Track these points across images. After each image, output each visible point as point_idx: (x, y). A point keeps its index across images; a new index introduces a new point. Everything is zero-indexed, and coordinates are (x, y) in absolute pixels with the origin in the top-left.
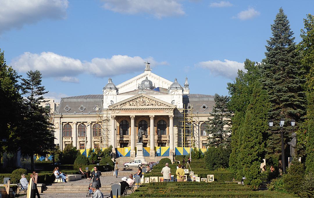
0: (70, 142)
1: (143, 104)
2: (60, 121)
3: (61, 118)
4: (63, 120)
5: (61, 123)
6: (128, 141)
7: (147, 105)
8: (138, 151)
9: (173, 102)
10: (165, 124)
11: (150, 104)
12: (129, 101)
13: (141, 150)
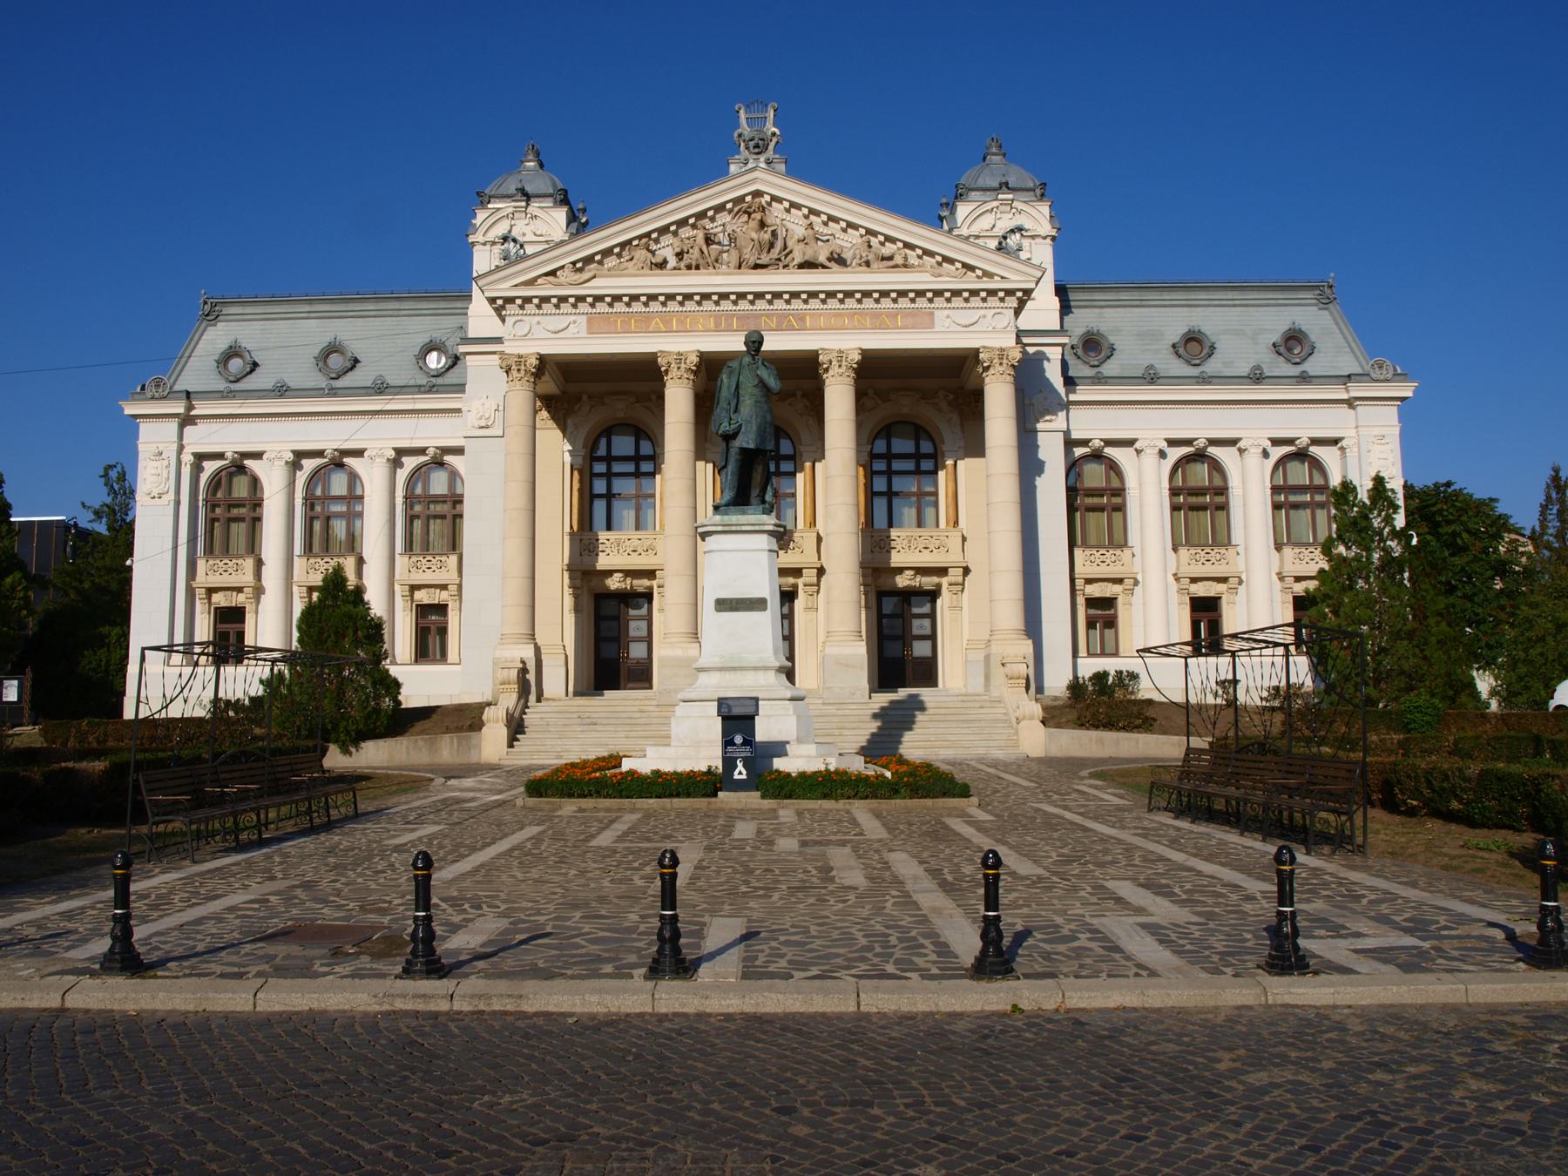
0: (239, 590)
1: (765, 260)
2: (181, 448)
3: (187, 420)
4: (201, 438)
5: (187, 458)
6: (650, 574)
7: (801, 266)
8: (724, 605)
9: (1013, 240)
10: (926, 447)
11: (822, 259)
12: (648, 235)
13: (757, 604)
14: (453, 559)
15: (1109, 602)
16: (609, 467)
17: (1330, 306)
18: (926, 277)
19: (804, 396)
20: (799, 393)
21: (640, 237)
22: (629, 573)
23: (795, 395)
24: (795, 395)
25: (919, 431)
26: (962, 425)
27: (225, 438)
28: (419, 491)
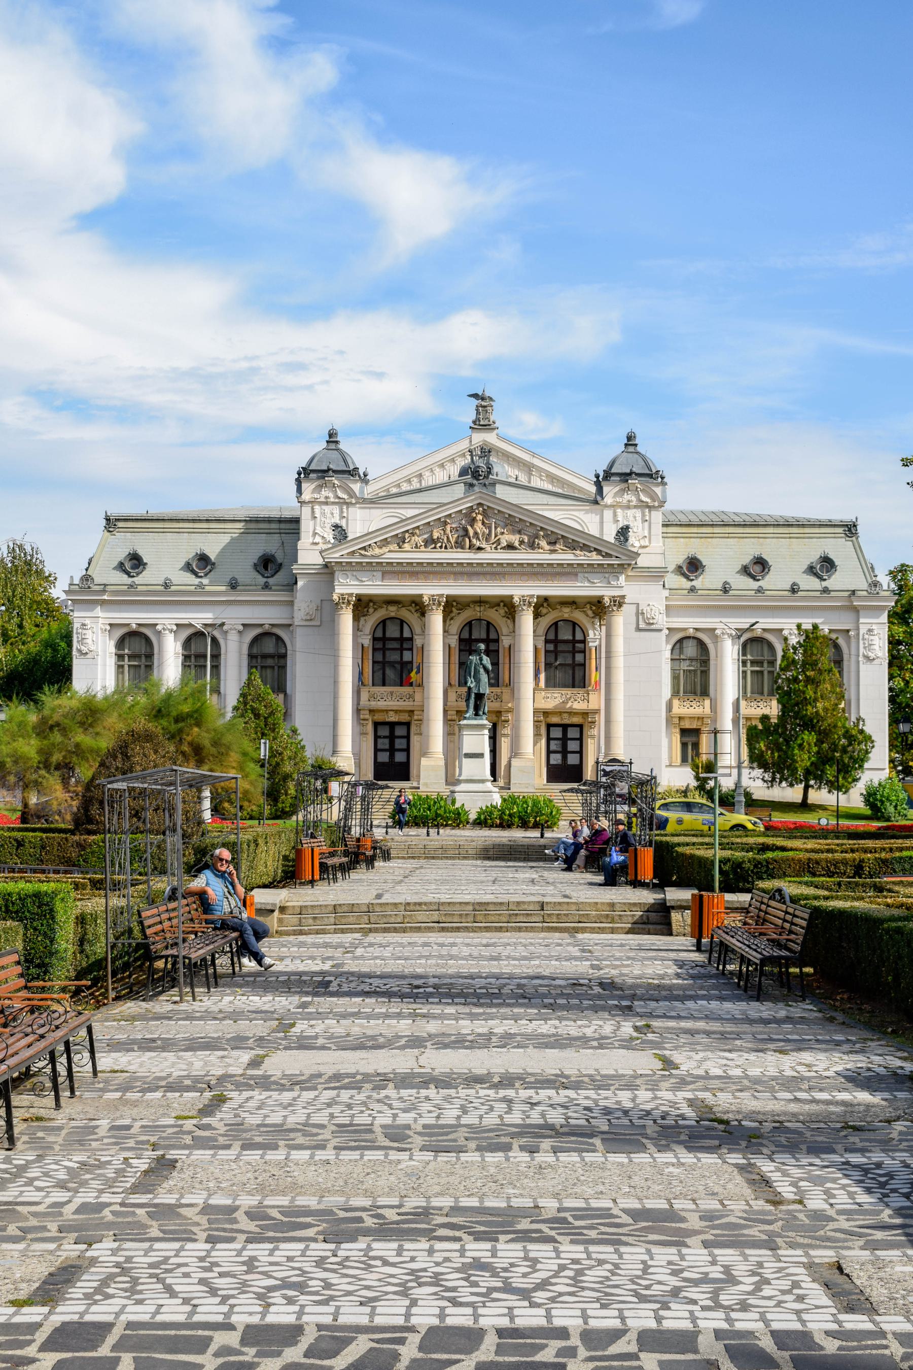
6: (412, 711)
10: (579, 636)
11: (517, 544)
14: (281, 696)
15: (696, 732)
16: (384, 645)
17: (854, 538)
18: (571, 557)
19: (504, 606)
20: (502, 604)
21: (414, 528)
22: (396, 711)
23: (499, 605)
24: (499, 605)
25: (574, 624)
26: (600, 625)
27: (133, 618)
28: (255, 651)
